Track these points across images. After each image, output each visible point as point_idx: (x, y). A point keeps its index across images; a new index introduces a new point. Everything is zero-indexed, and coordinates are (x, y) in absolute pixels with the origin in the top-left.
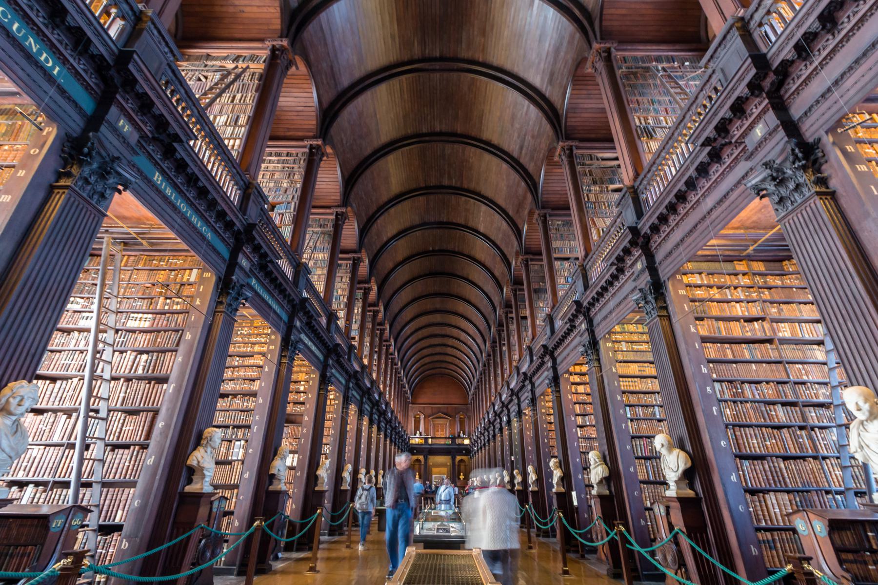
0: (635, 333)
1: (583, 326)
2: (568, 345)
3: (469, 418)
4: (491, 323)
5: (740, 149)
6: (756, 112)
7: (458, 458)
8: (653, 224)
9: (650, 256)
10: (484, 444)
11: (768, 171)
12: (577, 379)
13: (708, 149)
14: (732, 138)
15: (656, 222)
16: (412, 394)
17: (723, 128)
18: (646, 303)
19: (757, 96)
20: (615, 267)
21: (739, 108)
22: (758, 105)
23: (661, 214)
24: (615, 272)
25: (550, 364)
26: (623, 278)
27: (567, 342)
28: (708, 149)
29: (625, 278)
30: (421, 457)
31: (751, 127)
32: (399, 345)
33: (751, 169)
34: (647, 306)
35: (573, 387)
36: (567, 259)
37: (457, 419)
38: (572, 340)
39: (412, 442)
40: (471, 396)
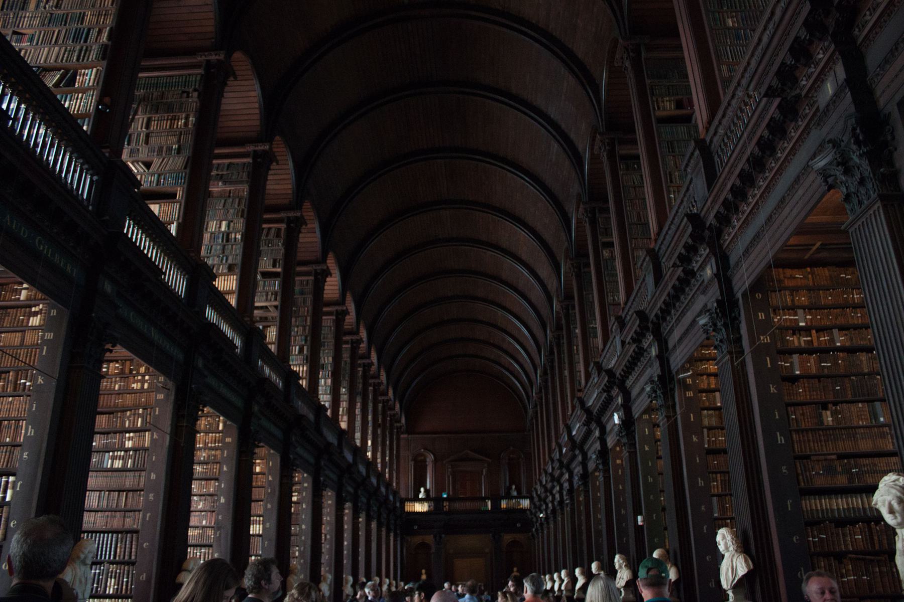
7: (507, 538)
10: (561, 502)
30: (429, 539)
40: (530, 412)
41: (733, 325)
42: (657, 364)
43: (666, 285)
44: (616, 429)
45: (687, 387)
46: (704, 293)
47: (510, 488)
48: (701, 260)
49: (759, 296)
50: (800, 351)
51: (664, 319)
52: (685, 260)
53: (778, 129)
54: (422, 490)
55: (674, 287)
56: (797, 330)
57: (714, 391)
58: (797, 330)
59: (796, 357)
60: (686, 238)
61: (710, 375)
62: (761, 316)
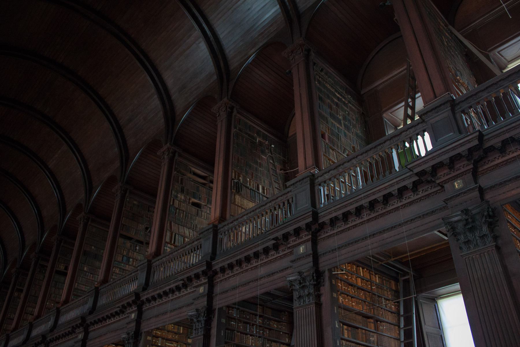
0: (172, 332)
1: (133, 316)
2: (109, 324)
5: (289, 251)
6: (305, 238)
8: (223, 266)
9: (211, 285)
11: (299, 277)
13: (274, 242)
14: (288, 244)
15: (226, 266)
17: (286, 237)
18: (198, 321)
19: (307, 231)
20: (182, 282)
21: (297, 232)
22: (306, 236)
23: (232, 263)
24: (181, 285)
25: (81, 336)
26: (184, 292)
27: (108, 322)
28: (274, 242)
29: (186, 292)
31: (299, 244)
33: (291, 267)
34: (197, 324)
36: (130, 239)
38: (114, 322)
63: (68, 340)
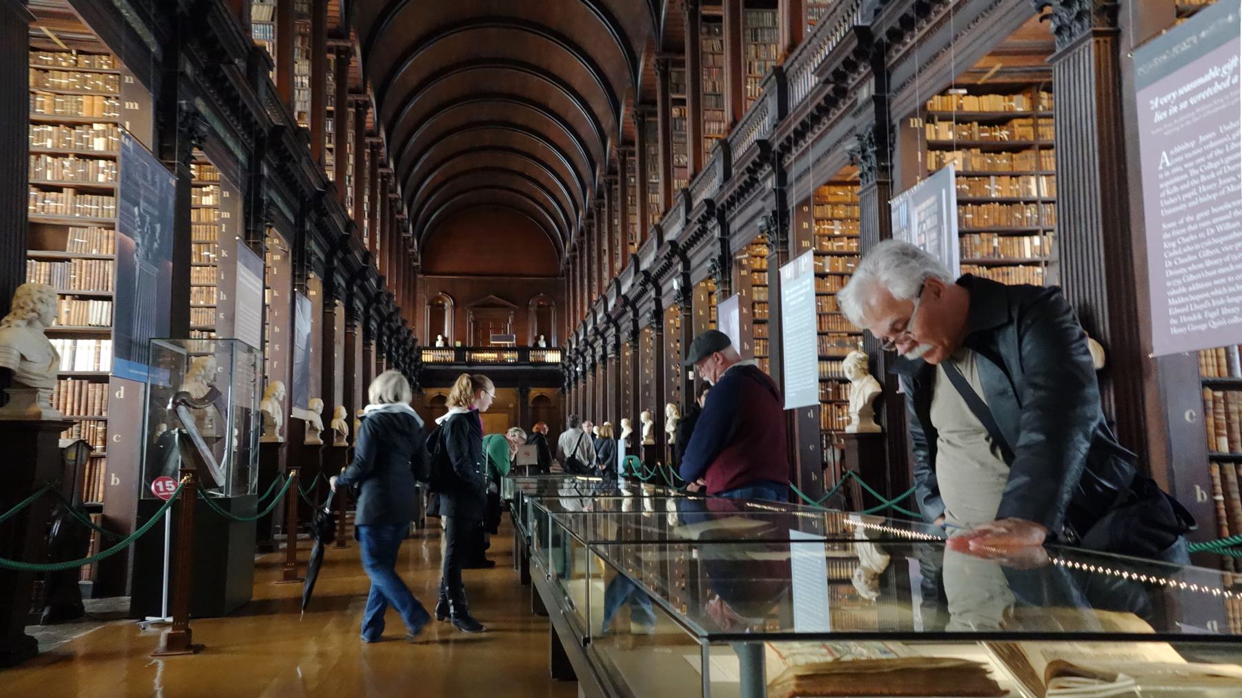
3: (561, 307)
4: (640, 48)
7: (534, 392)
10: (604, 357)
12: (946, 132)
16: (422, 249)
32: (390, 114)
35: (933, 155)
37: (532, 309)
39: (427, 357)
41: (784, 230)
42: (718, 245)
43: (733, 185)
44: (675, 293)
45: (742, 267)
46: (764, 200)
47: (538, 339)
48: (764, 174)
49: (806, 209)
50: (832, 254)
51: (729, 208)
52: (752, 171)
53: (831, 102)
54: (439, 337)
55: (740, 187)
56: (831, 237)
57: (764, 271)
58: (831, 237)
59: (828, 258)
60: (755, 157)
61: (762, 257)
62: (805, 225)
63: (831, 126)
